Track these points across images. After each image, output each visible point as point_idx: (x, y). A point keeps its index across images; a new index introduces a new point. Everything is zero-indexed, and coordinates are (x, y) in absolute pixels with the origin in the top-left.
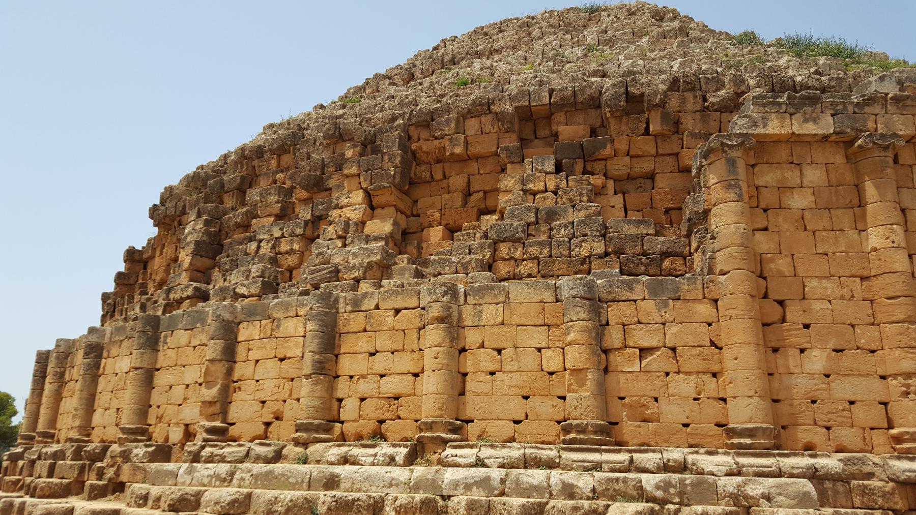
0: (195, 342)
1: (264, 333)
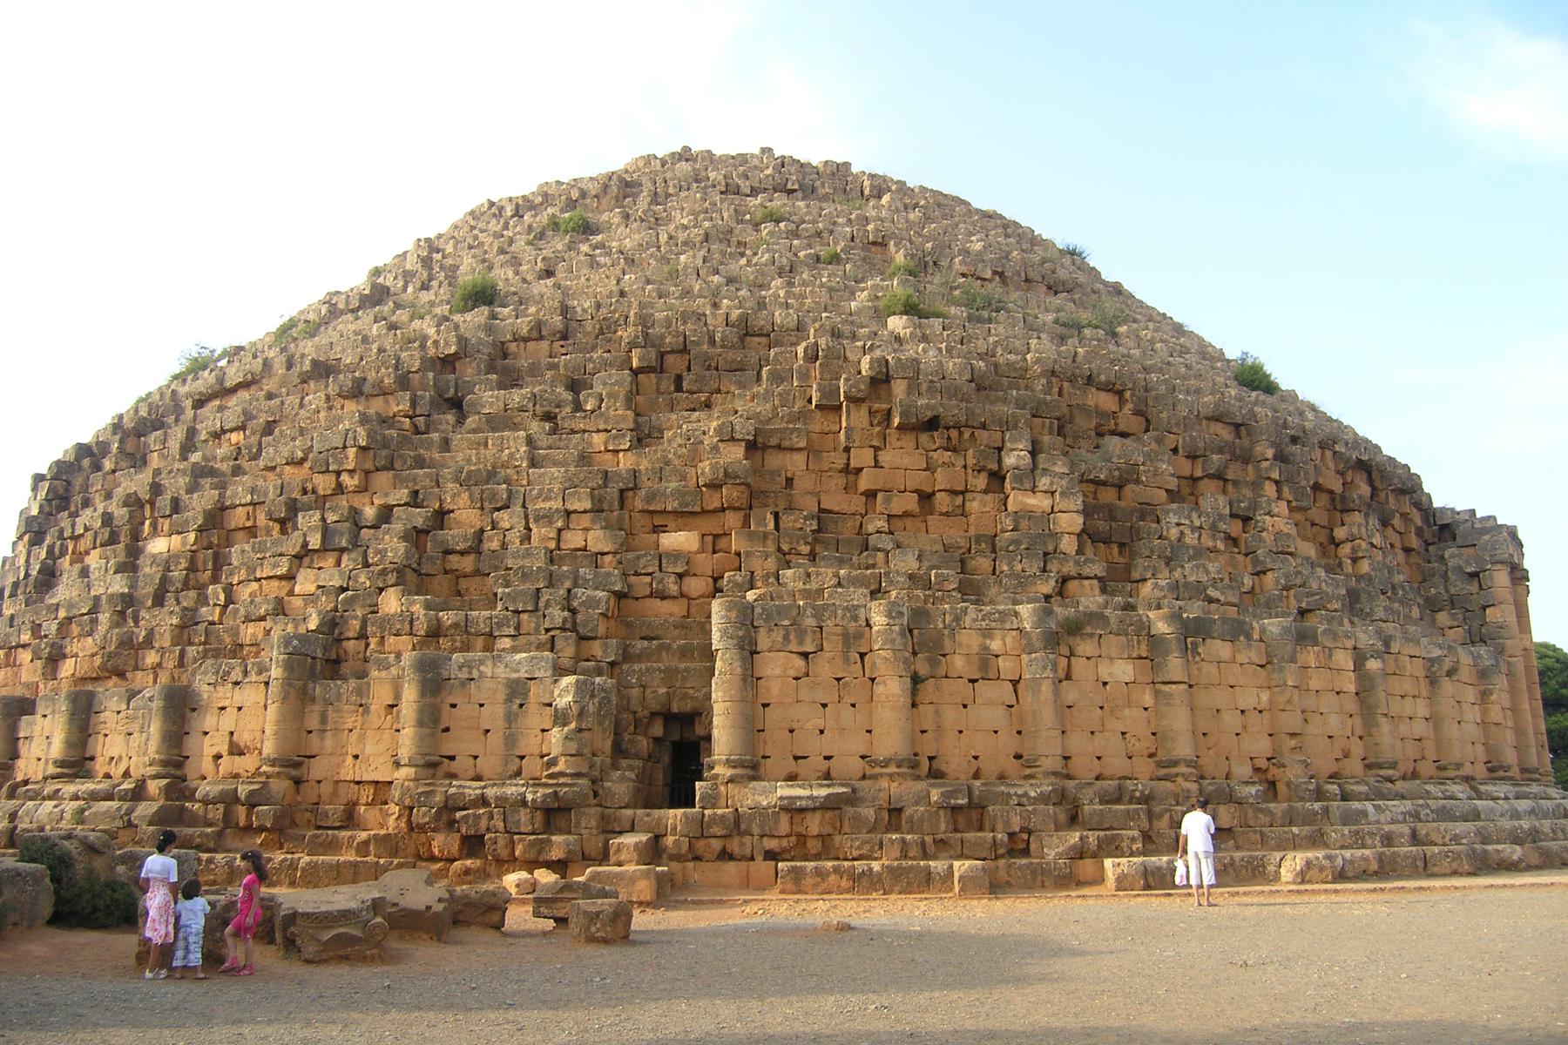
0: (1241, 658)
1: (1320, 662)
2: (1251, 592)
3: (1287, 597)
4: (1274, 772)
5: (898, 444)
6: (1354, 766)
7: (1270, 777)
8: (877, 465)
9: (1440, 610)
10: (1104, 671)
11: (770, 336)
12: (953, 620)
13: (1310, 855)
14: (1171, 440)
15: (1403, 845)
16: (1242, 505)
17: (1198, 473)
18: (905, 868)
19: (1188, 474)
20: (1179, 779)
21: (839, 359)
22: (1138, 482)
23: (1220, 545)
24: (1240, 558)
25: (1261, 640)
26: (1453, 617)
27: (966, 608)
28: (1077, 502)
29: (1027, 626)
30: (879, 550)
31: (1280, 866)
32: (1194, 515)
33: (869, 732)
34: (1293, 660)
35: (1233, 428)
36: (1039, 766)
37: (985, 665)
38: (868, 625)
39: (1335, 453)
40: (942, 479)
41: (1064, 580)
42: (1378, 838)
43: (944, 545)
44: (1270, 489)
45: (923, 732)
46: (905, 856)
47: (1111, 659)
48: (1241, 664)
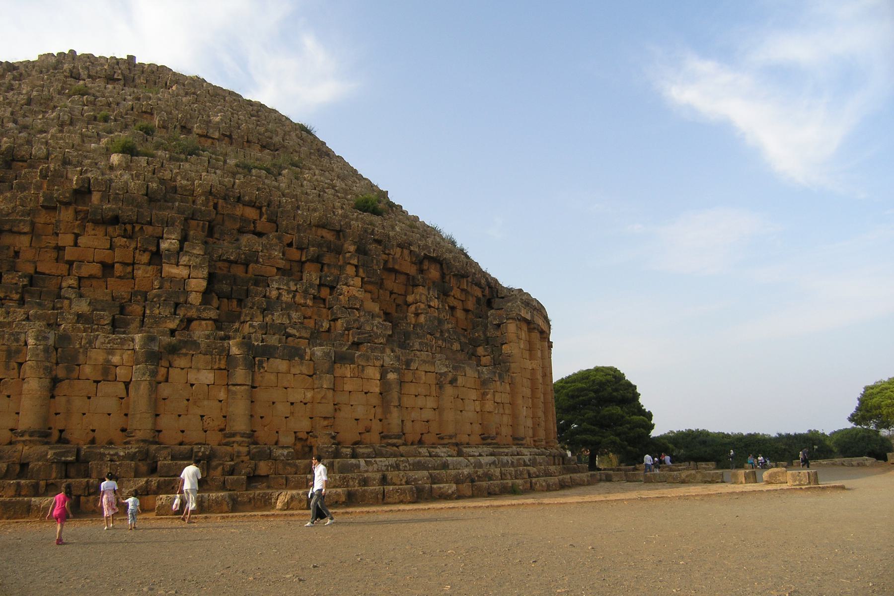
2: (329, 330)
3: (348, 335)
4: (311, 440)
5: (93, 232)
6: (374, 437)
7: (308, 443)
8: (76, 244)
9: (479, 346)
10: (192, 377)
11: (31, 162)
12: (87, 343)
13: (294, 492)
14: (287, 238)
15: (374, 485)
16: (328, 278)
17: (304, 259)
18: (14, 502)
19: (298, 258)
20: (235, 445)
21: (62, 177)
22: (257, 262)
23: (310, 303)
24: (324, 310)
25: (311, 360)
26: (486, 350)
27: (98, 335)
28: (205, 273)
29: (137, 347)
30: (67, 298)
31: (277, 499)
32: (292, 284)
33: (18, 413)
34: (331, 371)
35: (335, 233)
36: (133, 436)
37: (107, 372)
38: (26, 344)
39: (411, 251)
40: (118, 255)
41: (190, 321)
42: (357, 481)
43: (113, 296)
44: (350, 270)
45: (56, 414)
46: (18, 494)
47: (199, 370)
48: (294, 374)
